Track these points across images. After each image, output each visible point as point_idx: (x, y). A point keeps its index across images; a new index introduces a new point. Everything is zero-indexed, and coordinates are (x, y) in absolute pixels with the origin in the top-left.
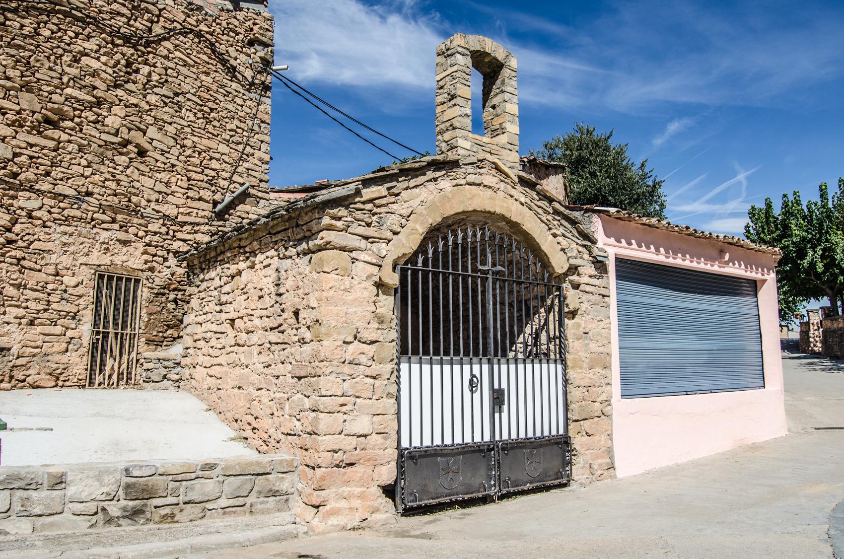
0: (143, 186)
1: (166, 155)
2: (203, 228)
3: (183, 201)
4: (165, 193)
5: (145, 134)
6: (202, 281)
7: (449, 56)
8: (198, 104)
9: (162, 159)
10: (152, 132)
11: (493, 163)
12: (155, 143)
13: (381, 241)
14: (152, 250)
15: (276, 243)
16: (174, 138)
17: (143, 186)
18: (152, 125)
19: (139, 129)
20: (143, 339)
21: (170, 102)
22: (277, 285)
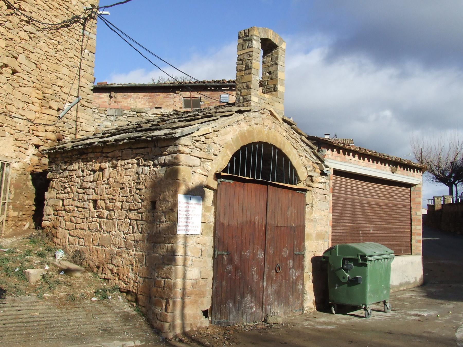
0: (15, 98)
1: (30, 75)
2: (50, 128)
3: (39, 109)
4: (28, 103)
5: (16, 58)
6: (65, 170)
7: (246, 40)
8: (51, 39)
9: (27, 78)
10: (22, 58)
11: (270, 111)
12: (23, 67)
13: (208, 160)
14: (19, 144)
15: (137, 155)
16: (35, 64)
17: (15, 98)
18: (21, 53)
19: (14, 57)
20: (11, 206)
21: (34, 37)
22: (138, 183)
